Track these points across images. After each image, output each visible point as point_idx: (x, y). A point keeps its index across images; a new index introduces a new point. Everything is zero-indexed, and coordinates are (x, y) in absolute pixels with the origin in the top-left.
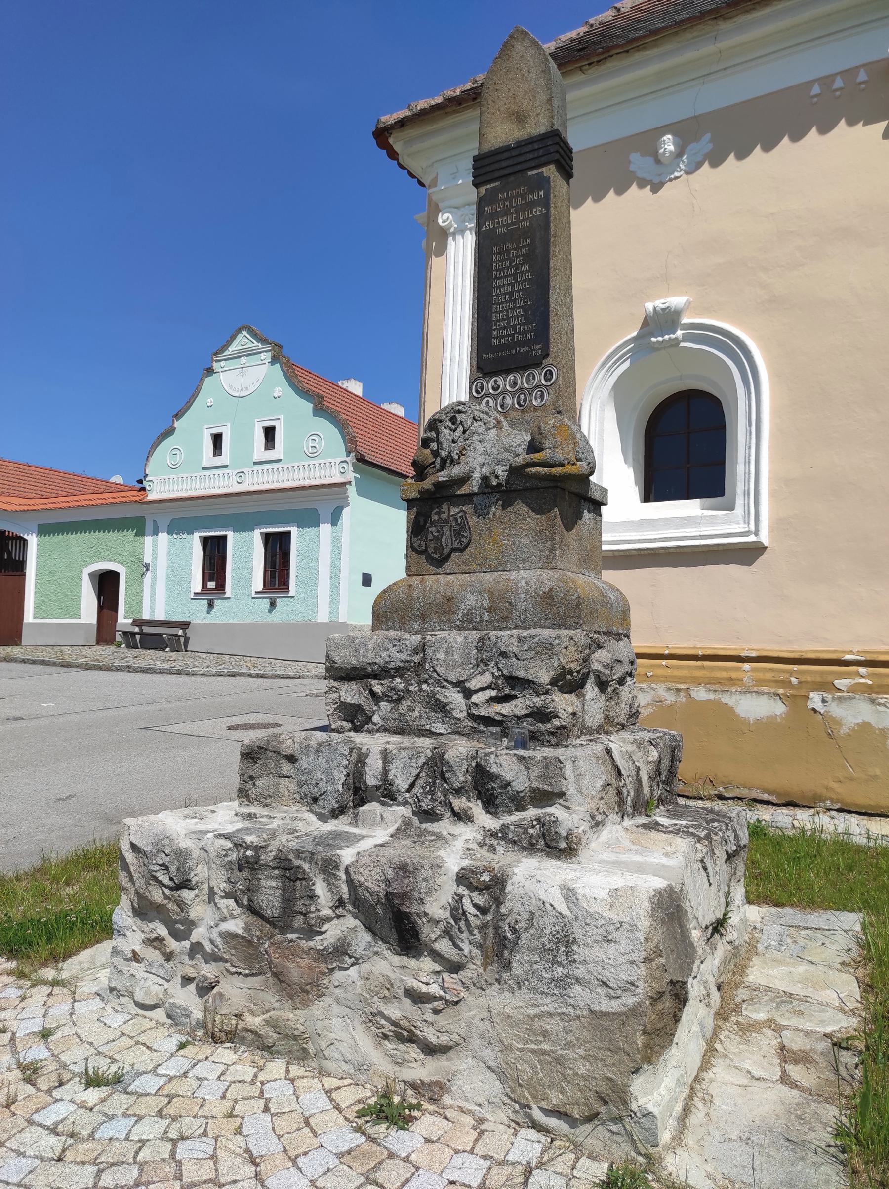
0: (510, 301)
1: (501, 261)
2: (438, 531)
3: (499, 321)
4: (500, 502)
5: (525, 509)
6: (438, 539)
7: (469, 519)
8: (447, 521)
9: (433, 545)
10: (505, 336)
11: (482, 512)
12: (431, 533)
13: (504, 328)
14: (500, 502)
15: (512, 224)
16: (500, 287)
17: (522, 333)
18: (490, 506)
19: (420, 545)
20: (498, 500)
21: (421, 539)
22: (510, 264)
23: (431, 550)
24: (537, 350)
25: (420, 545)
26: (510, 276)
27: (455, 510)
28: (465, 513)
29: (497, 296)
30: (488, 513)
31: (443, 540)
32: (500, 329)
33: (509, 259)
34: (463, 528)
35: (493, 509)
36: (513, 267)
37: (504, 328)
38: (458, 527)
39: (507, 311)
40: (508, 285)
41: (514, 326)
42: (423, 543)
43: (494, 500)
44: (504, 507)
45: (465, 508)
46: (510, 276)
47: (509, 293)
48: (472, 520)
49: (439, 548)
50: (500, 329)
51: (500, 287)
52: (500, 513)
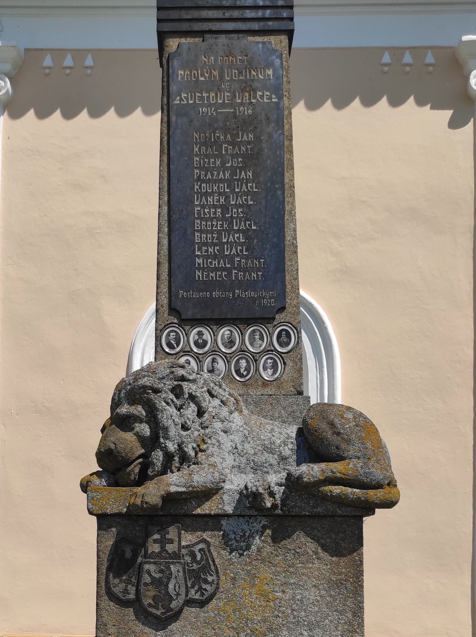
0: (224, 219)
1: (207, 156)
2: (161, 571)
3: (206, 244)
4: (269, 532)
5: (311, 546)
6: (160, 584)
7: (215, 554)
8: (176, 556)
9: (152, 593)
10: (216, 269)
11: (237, 544)
12: (149, 572)
13: (215, 257)
14: (269, 532)
15: (223, 105)
16: (206, 194)
17: (245, 270)
18: (252, 536)
19: (126, 591)
20: (264, 528)
21: (128, 582)
22: (223, 163)
23: (147, 601)
24: (268, 300)
25: (126, 591)
26: (221, 181)
27: (188, 538)
28: (208, 544)
29: (203, 207)
30: (248, 547)
31: (171, 586)
32: (208, 257)
33: (220, 156)
34: (205, 569)
35: (257, 541)
36: (227, 169)
37: (215, 257)
38: (195, 566)
39: (219, 232)
40: (220, 194)
41: (231, 258)
42: (132, 590)
43: (258, 527)
44: (276, 539)
45: (206, 535)
46: (221, 181)
47: (222, 206)
48: (220, 556)
49: (164, 598)
50: (208, 257)
51: (206, 194)
52: (268, 549)
